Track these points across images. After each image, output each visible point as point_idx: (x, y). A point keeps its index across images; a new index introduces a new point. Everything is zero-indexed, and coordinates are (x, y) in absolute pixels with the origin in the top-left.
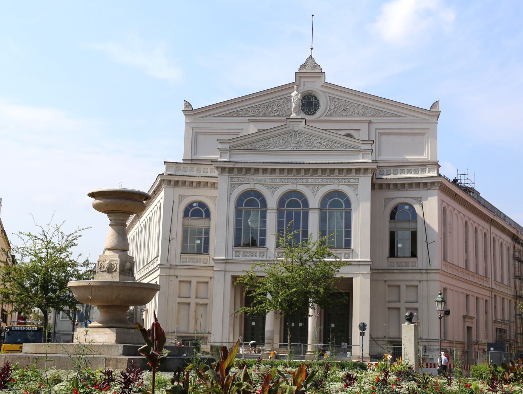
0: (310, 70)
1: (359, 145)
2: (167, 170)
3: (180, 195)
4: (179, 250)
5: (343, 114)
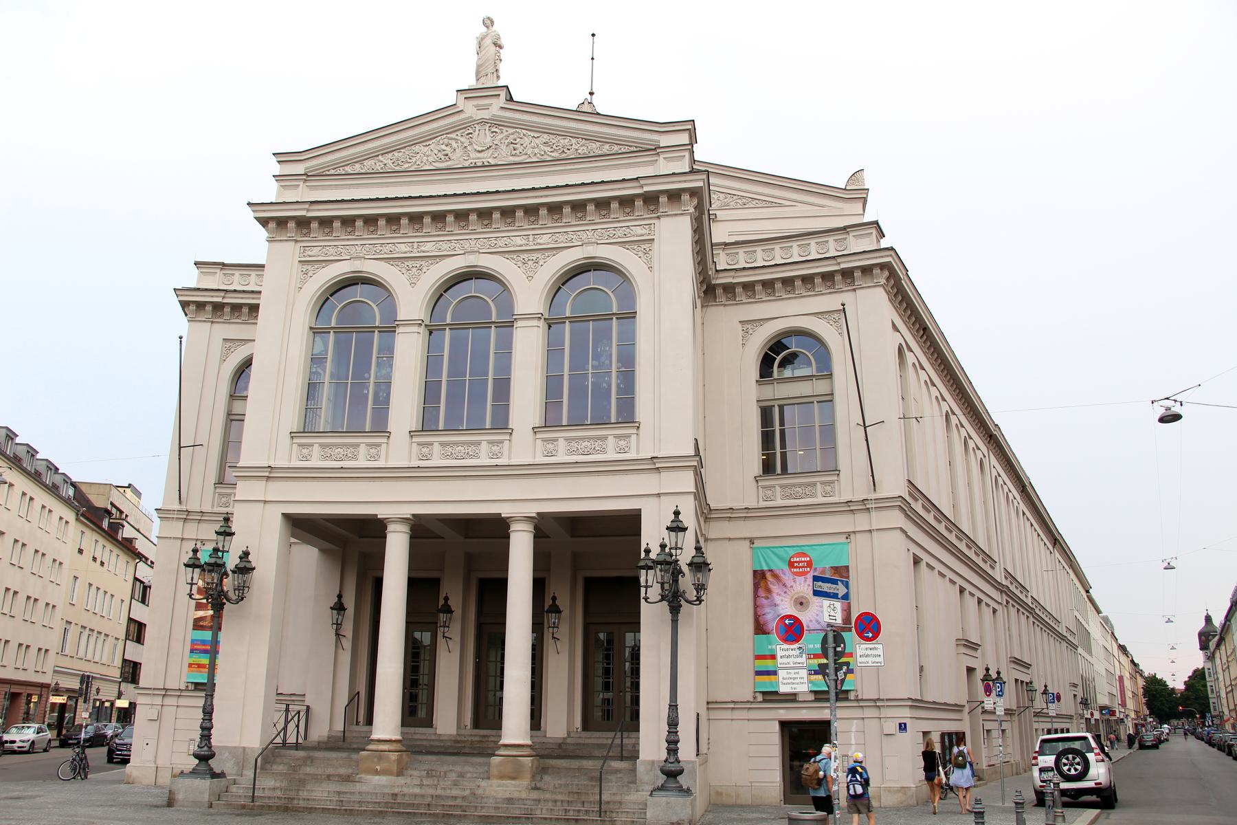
2: (198, 282)
4: (212, 477)
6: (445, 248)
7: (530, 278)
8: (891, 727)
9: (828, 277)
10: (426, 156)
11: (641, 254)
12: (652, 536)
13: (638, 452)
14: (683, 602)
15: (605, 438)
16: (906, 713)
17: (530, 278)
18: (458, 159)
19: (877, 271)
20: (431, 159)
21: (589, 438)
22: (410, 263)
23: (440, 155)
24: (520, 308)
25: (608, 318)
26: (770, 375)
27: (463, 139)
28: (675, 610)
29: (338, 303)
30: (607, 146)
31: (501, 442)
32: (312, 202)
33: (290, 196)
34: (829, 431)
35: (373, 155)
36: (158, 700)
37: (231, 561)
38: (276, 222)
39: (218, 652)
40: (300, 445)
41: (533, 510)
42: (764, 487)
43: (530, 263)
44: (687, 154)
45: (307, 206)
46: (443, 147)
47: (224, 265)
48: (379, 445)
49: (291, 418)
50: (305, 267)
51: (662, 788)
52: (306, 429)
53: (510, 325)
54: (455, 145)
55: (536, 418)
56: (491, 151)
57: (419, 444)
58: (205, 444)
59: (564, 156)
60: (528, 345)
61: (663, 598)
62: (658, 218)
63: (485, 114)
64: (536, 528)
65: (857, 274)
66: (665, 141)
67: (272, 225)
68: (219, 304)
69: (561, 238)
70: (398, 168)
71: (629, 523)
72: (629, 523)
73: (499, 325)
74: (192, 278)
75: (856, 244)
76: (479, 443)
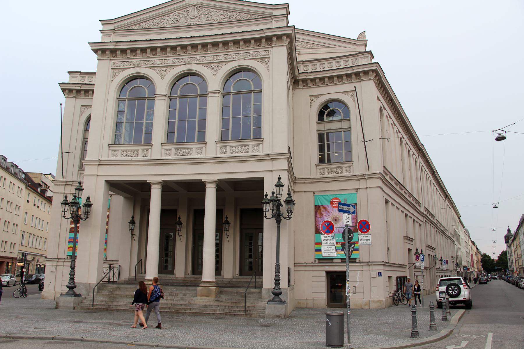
1: (271, 11)
2: (70, 79)
4: (77, 166)
6: (177, 62)
8: (375, 274)
9: (348, 76)
10: (168, 21)
11: (264, 64)
12: (269, 189)
13: (262, 152)
14: (282, 218)
15: (248, 146)
16: (381, 268)
18: (182, 22)
19: (370, 73)
20: (170, 22)
21: (241, 146)
22: (161, 69)
23: (174, 20)
24: (210, 88)
25: (250, 92)
26: (323, 119)
27: (185, 13)
28: (279, 222)
29: (129, 87)
30: (249, 16)
31: (202, 148)
32: (117, 42)
33: (107, 39)
34: (349, 144)
35: (144, 21)
36: (55, 263)
37: (82, 201)
38: (101, 51)
39: (77, 242)
40: (113, 150)
41: (216, 178)
42: (320, 169)
43: (215, 68)
44: (285, 19)
45: (115, 44)
46: (176, 17)
47: (81, 73)
48: (148, 150)
49: (109, 138)
50: (115, 71)
51: (272, 300)
52: (116, 143)
53: (206, 96)
54: (181, 16)
55: (218, 137)
56: (197, 19)
57: (165, 149)
58: (74, 152)
59: (230, 20)
60: (214, 105)
61: (273, 216)
62: (272, 47)
64: (217, 186)
65: (362, 74)
66: (275, 13)
67: (99, 52)
68: (78, 89)
69: (229, 57)
70: (156, 27)
71: (259, 183)
72: (259, 183)
73: (201, 96)
74: (66, 79)
75: (361, 61)
76: (192, 148)
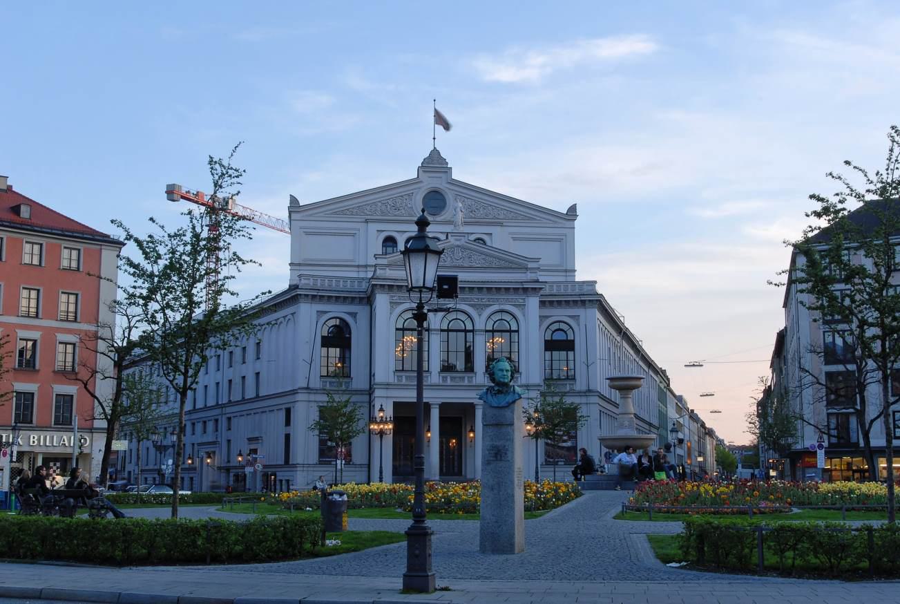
0: (435, 163)
1: (526, 262)
3: (317, 311)
5: (473, 216)
7: (480, 315)
17: (480, 315)
19: (595, 302)
63: (458, 243)
66: (530, 265)
